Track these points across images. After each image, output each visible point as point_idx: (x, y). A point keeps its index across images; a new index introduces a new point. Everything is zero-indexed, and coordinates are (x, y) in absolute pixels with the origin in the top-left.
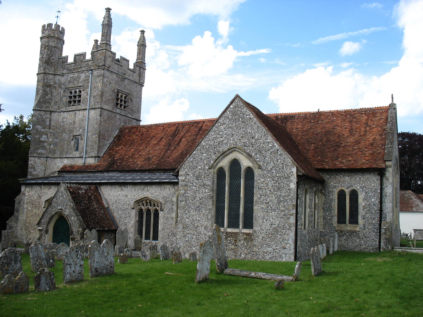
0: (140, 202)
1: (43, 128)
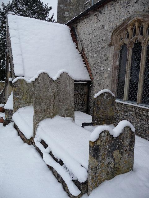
0: (123, 30)
1: (65, 6)
